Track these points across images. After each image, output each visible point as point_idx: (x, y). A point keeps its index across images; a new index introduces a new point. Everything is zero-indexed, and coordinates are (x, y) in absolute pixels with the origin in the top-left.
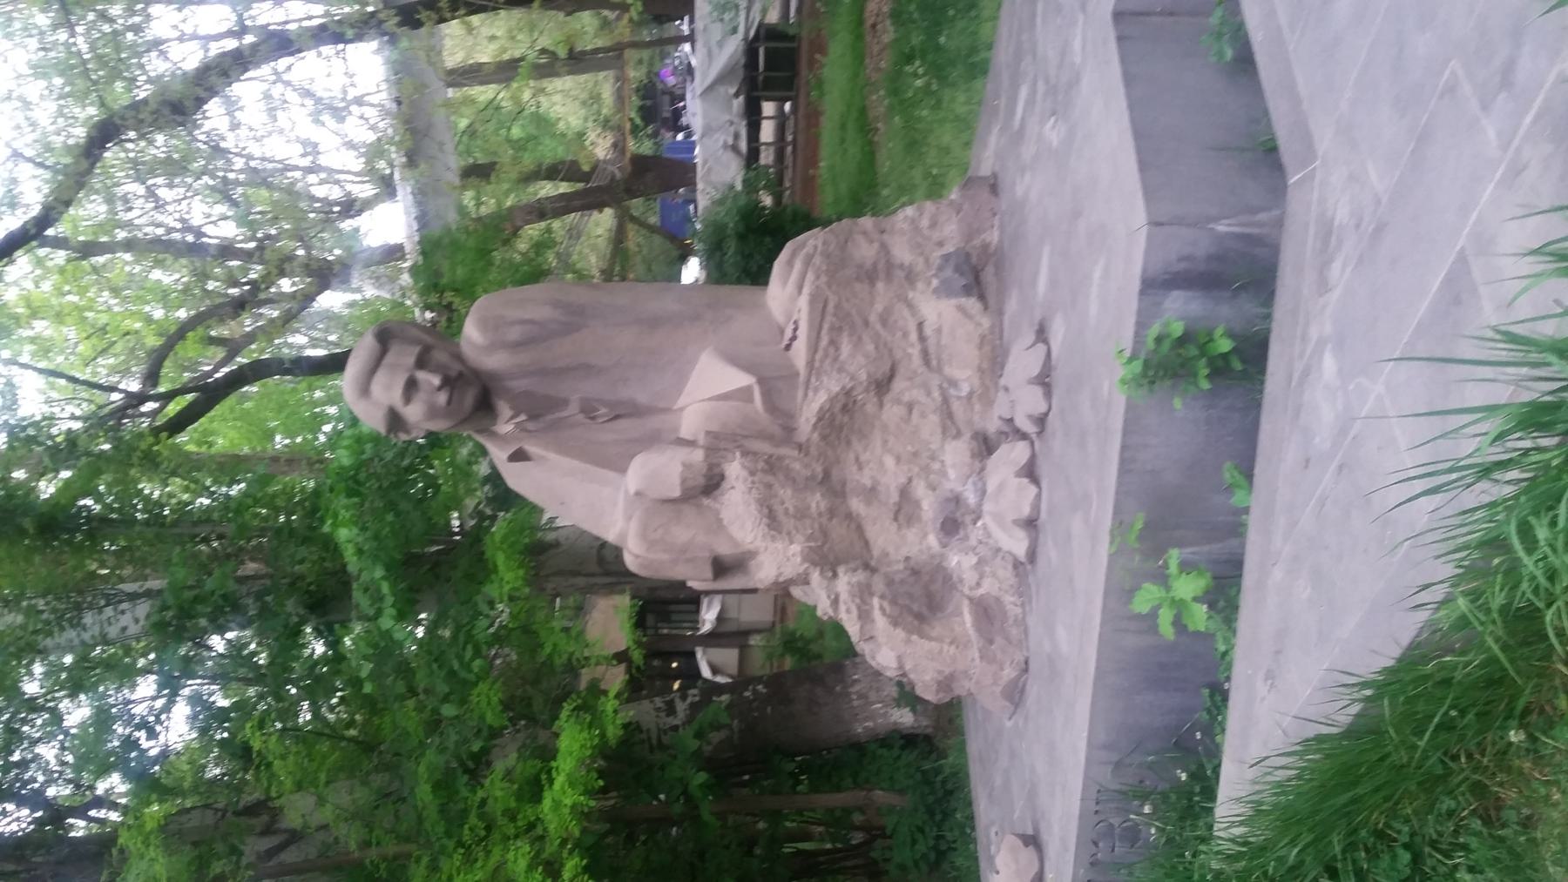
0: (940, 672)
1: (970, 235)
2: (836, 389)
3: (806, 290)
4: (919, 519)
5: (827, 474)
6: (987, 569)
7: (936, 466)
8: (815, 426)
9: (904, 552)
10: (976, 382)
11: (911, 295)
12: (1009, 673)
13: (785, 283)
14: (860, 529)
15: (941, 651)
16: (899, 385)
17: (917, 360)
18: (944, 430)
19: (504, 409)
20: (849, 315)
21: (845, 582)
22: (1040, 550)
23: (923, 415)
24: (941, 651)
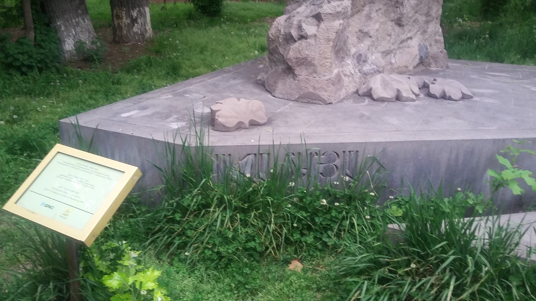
0: (314, 58)
1: (435, 58)
4: (359, 43)
6: (351, 79)
7: (374, 50)
9: (350, 36)
10: (396, 66)
11: (419, 33)
12: (324, 95)
14: (359, 11)
15: (326, 58)
16: (397, 28)
18: (383, 52)
24: (326, 58)
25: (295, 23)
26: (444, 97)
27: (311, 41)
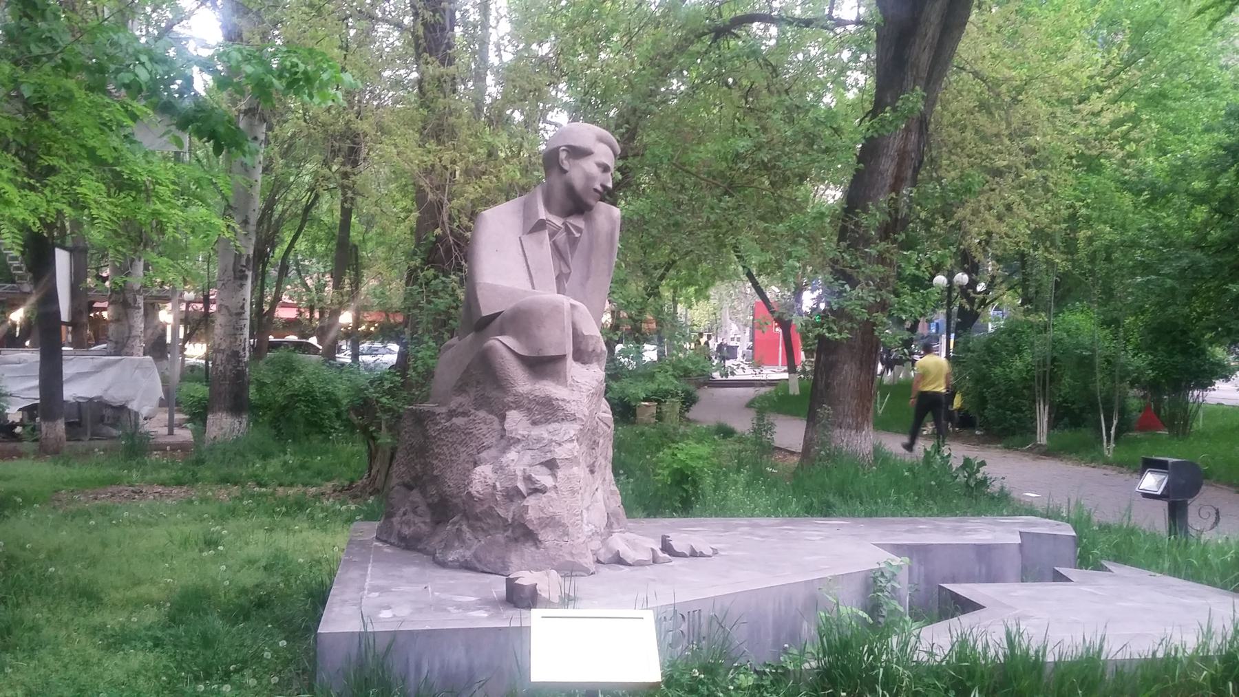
19: (579, 222)
22: (639, 573)
25: (519, 473)
26: (694, 554)
27: (552, 494)
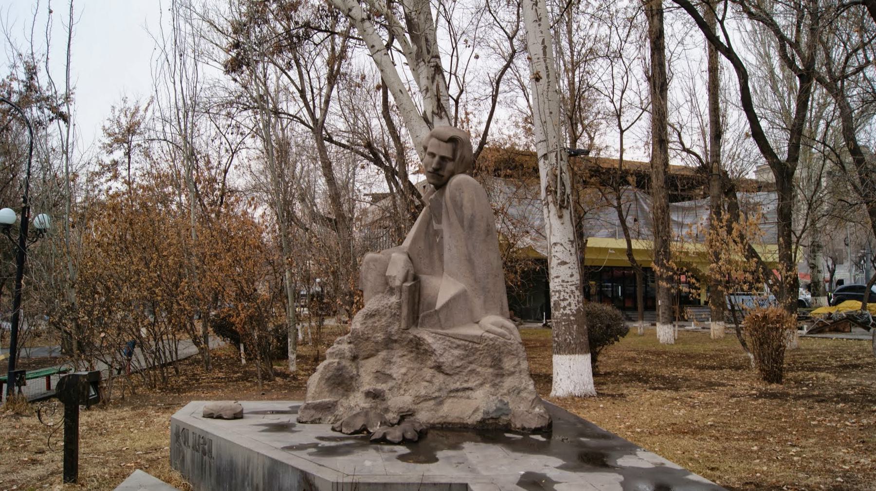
2: (434, 346)
3: (486, 334)
5: (396, 341)
8: (415, 336)
11: (488, 385)
13: (493, 324)
17: (453, 386)
20: (474, 354)
21: (345, 347)
23: (425, 387)
